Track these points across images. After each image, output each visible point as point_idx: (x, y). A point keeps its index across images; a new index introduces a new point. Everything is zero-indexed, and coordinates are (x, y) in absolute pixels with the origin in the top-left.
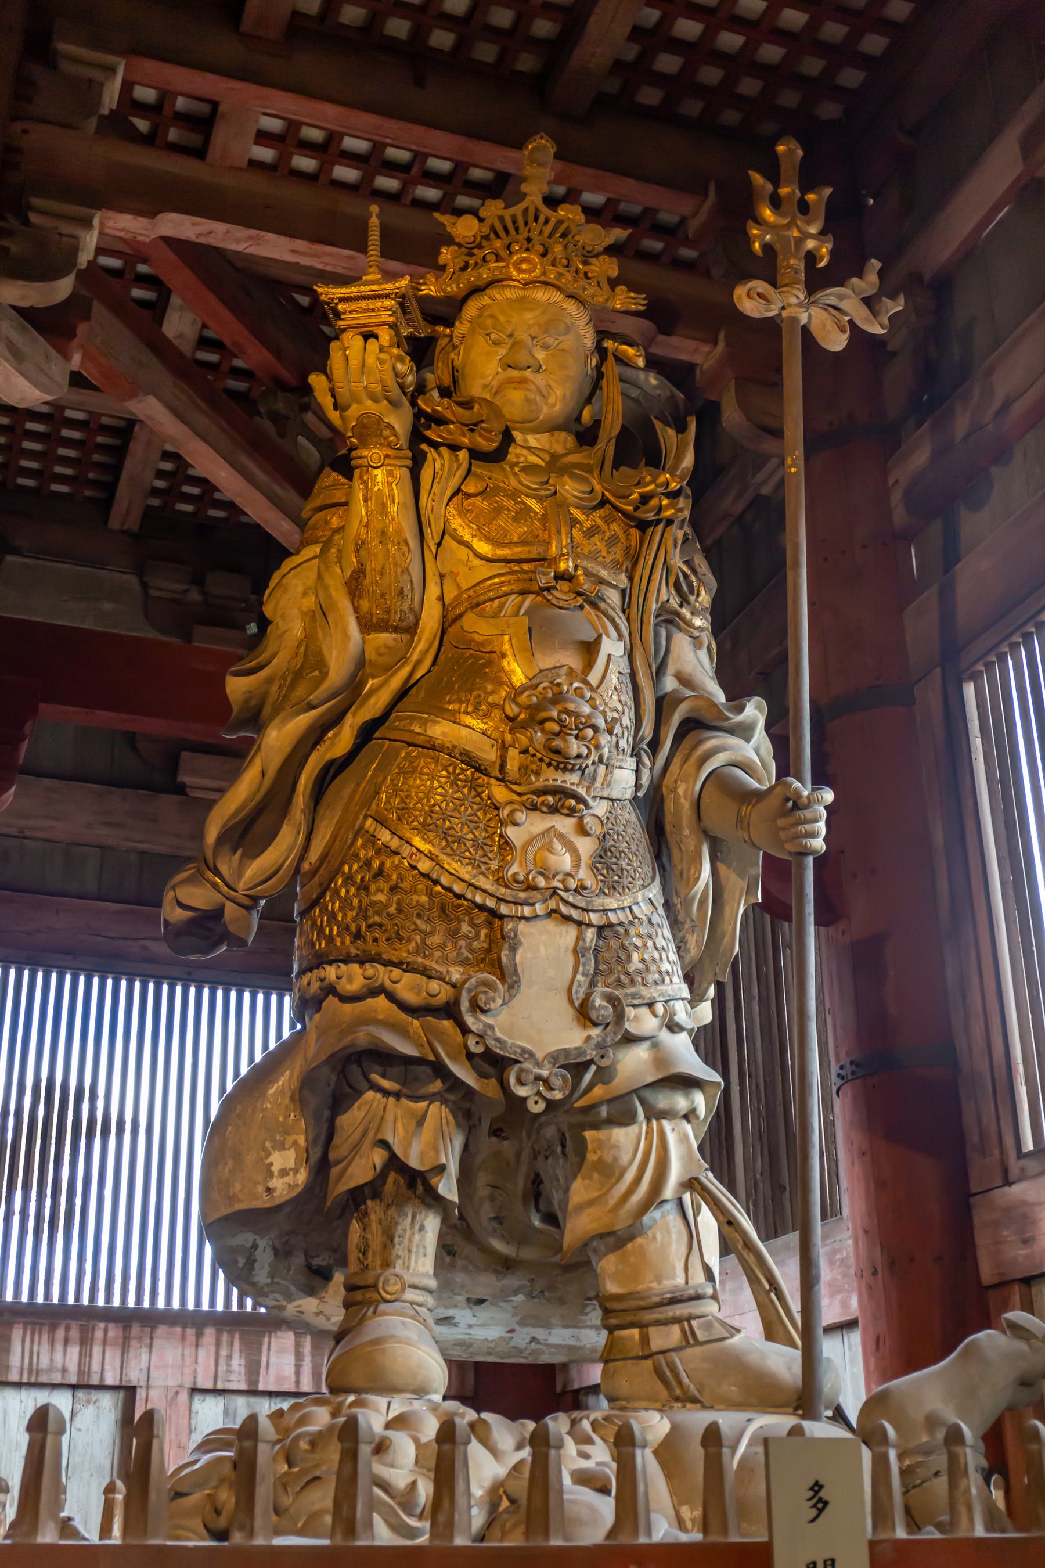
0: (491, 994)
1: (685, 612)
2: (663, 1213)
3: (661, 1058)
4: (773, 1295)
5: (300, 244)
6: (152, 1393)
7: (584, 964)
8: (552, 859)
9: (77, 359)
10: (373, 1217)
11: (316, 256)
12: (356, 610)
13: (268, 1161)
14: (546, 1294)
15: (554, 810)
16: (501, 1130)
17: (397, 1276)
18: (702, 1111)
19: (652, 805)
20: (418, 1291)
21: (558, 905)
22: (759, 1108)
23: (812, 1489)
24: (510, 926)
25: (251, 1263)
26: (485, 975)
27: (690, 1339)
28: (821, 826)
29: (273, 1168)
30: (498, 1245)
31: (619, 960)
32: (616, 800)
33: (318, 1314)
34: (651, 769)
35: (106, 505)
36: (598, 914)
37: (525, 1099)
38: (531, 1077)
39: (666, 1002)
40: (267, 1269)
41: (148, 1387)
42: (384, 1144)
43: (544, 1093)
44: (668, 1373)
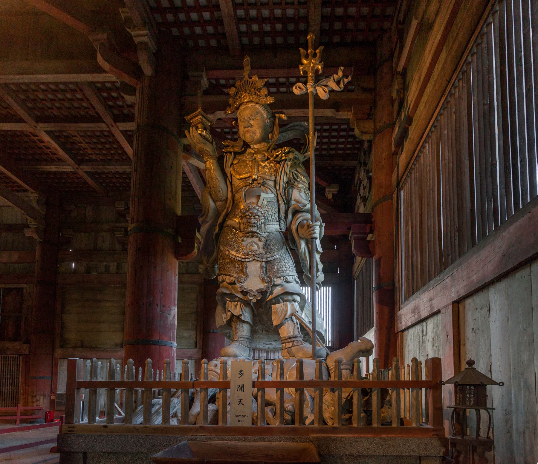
12: (212, 198)
15: (253, 237)
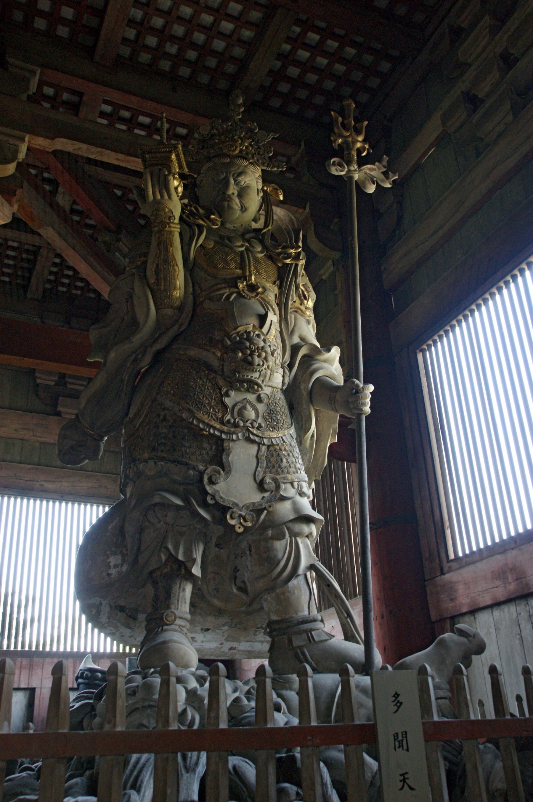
0: (218, 475)
1: (302, 307)
2: (298, 581)
3: (296, 508)
4: (348, 620)
5: (121, 156)
6: (43, 690)
7: (261, 463)
8: (246, 412)
9: (16, 207)
10: (160, 584)
11: (128, 162)
13: (109, 560)
14: (238, 626)
15: (248, 390)
16: (220, 544)
17: (172, 612)
18: (314, 534)
19: (290, 392)
20: (182, 620)
21: (249, 435)
22: (324, 549)
23: (394, 696)
24: (227, 444)
25: (99, 612)
26: (214, 467)
27: (311, 640)
28: (368, 400)
29: (111, 564)
30: (217, 602)
31: (277, 462)
32: (275, 387)
33: (130, 637)
34: (289, 376)
35: (26, 288)
36: (267, 439)
37: (234, 526)
38: (237, 515)
39: (298, 482)
40: (107, 615)
41: (41, 688)
42: (167, 549)
43: (243, 523)
44: (302, 657)
